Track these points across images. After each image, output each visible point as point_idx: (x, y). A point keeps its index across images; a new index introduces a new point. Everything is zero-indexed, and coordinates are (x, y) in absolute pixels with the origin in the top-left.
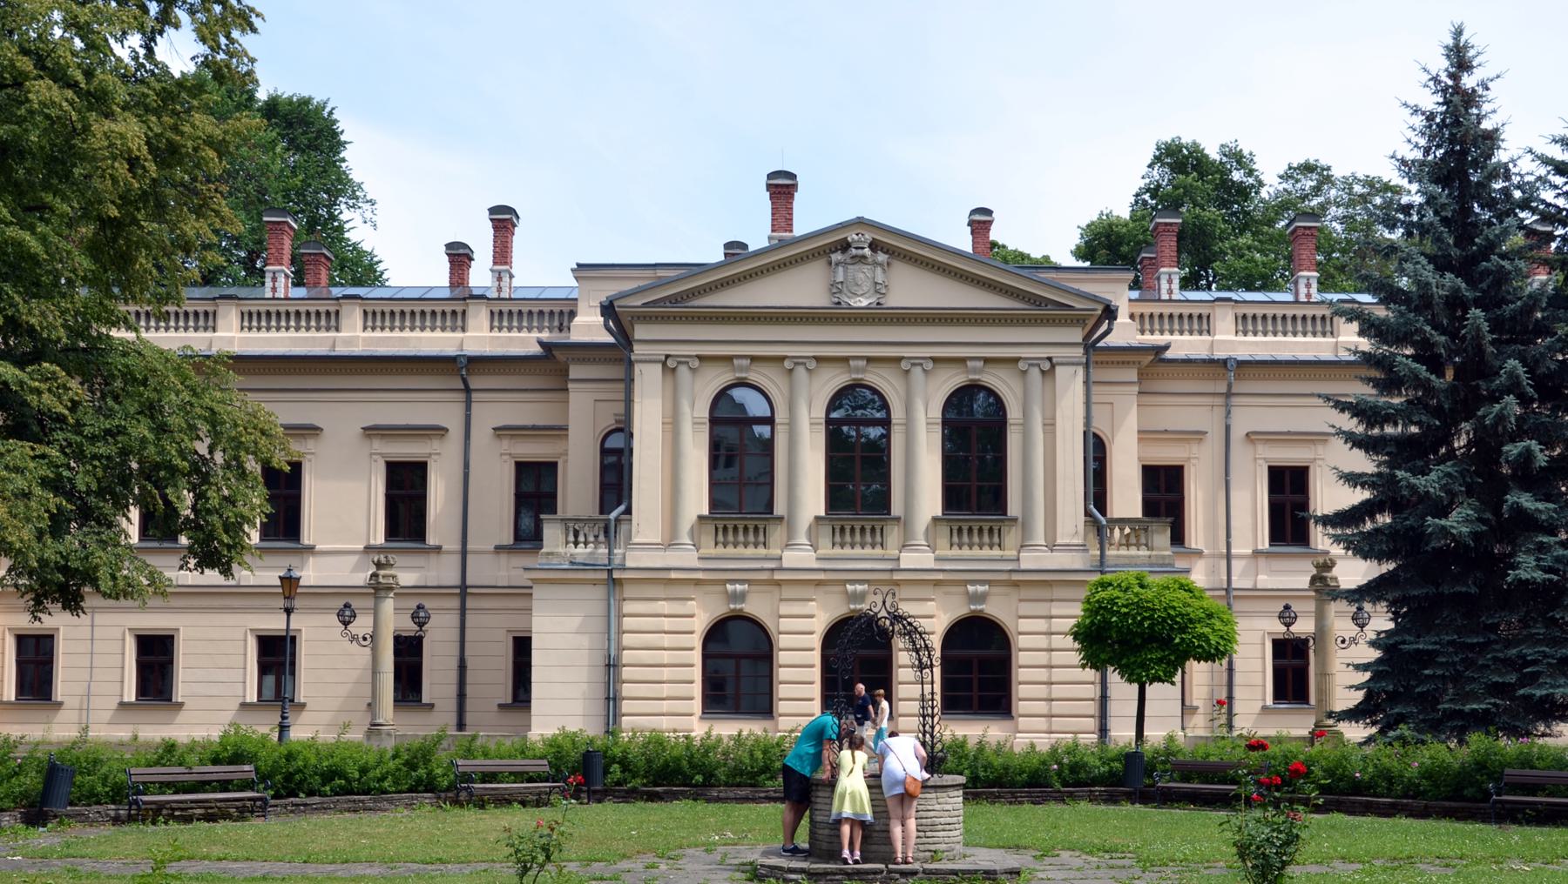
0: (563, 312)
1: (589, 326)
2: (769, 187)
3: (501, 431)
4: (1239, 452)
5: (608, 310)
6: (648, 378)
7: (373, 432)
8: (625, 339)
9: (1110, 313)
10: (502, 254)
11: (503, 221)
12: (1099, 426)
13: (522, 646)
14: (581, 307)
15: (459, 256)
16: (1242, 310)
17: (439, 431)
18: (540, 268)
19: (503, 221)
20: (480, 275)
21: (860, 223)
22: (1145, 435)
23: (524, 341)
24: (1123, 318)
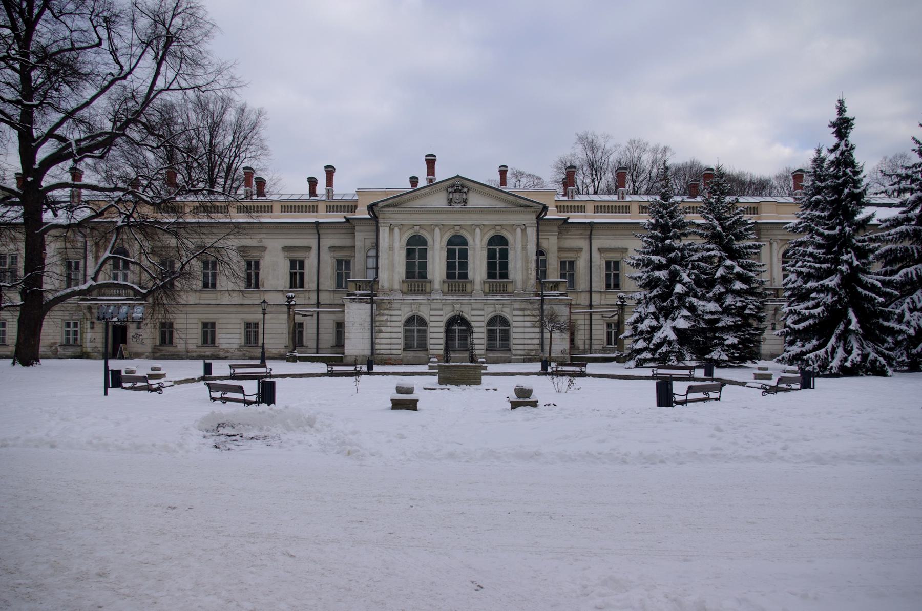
0: (353, 208)
1: (362, 213)
2: (426, 160)
3: (332, 248)
4: (596, 255)
5: (371, 208)
6: (384, 233)
7: (286, 249)
8: (375, 218)
9: (545, 208)
10: (329, 183)
11: (330, 171)
12: (544, 244)
13: (340, 327)
14: (359, 204)
15: (313, 182)
16: (597, 204)
17: (309, 248)
18: (344, 187)
19: (330, 171)
20: (321, 188)
21: (458, 176)
22: (560, 250)
23: (339, 218)
24: (552, 208)
